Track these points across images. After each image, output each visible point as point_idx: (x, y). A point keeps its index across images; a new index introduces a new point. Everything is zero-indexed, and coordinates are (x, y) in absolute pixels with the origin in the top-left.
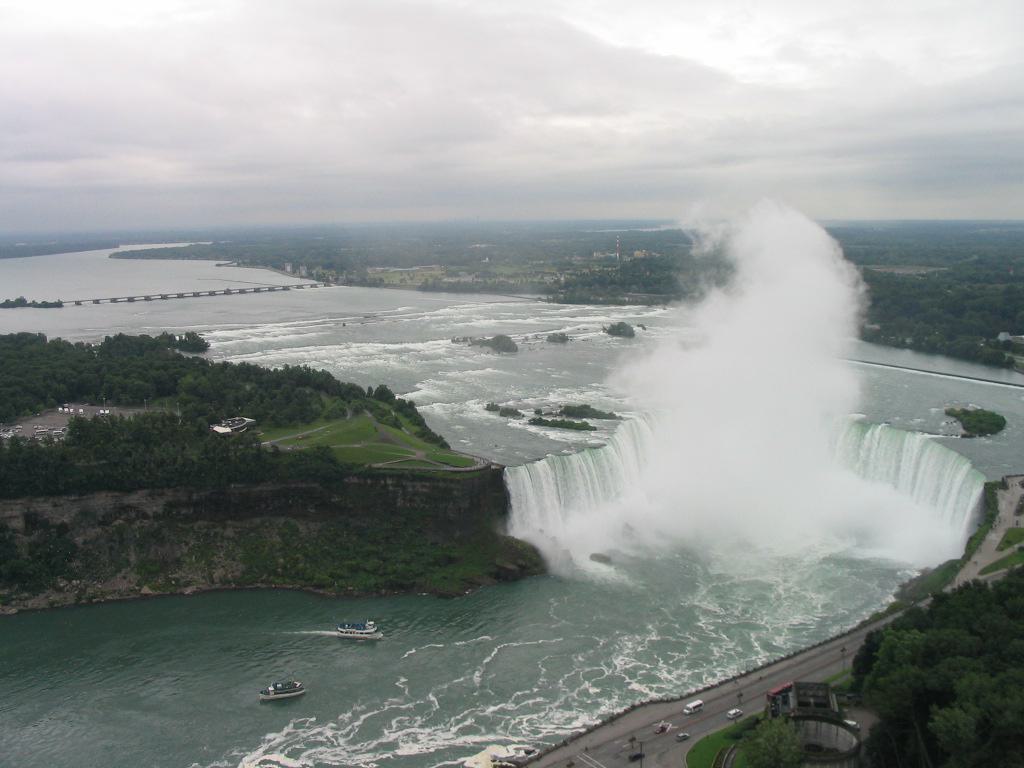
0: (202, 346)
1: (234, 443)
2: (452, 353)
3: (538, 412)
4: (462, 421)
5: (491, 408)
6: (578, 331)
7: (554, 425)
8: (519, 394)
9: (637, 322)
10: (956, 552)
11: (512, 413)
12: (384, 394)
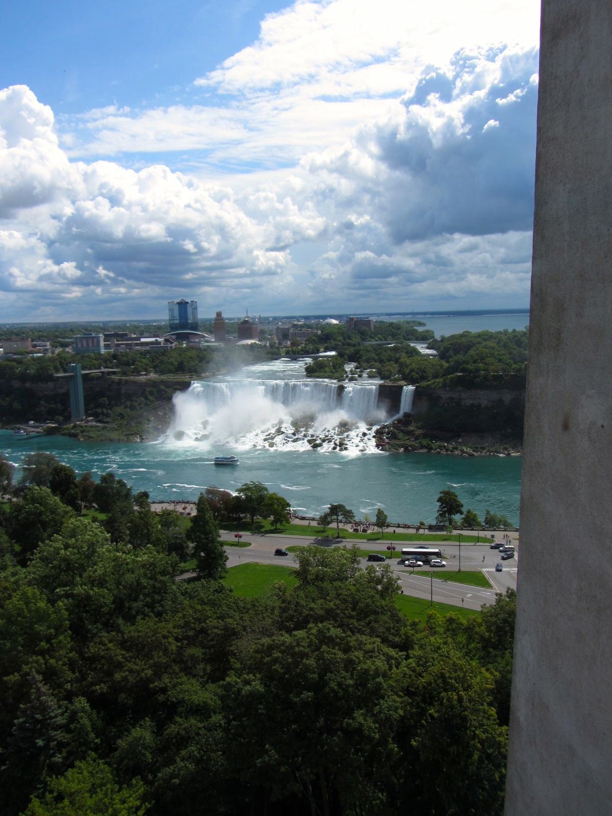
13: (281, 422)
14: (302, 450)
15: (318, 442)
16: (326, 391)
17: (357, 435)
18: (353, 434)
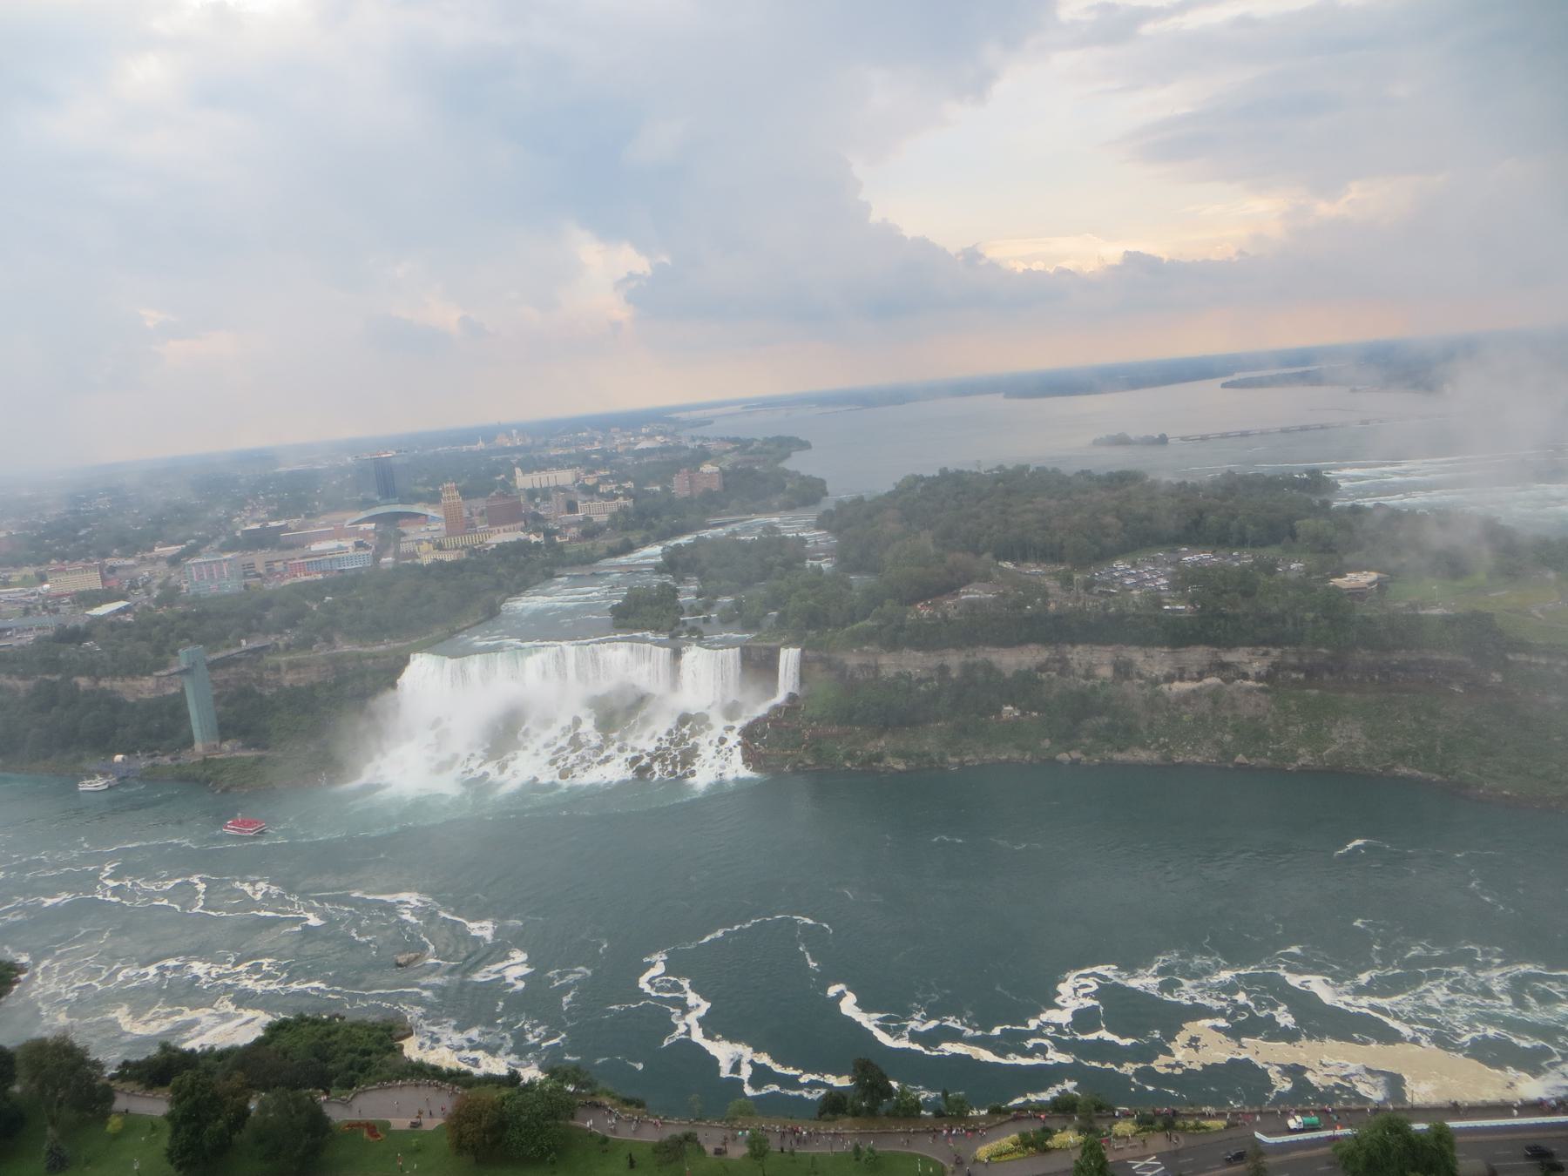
13: (577, 722)
14: (616, 778)
15: (643, 763)
16: (650, 660)
17: (710, 743)
18: (702, 740)
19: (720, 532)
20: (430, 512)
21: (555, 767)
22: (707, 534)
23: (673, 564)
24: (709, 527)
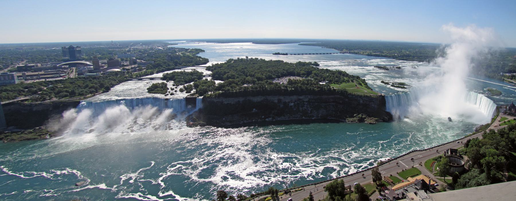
0: (318, 65)
1: (324, 86)
2: (373, 70)
3: (393, 84)
4: (376, 85)
5: (382, 82)
6: (403, 66)
7: (397, 87)
8: (389, 79)
9: (416, 65)
10: (489, 122)
11: (388, 84)
12: (358, 77)
19: (179, 70)
20: (88, 63)
21: (129, 129)
22: (176, 70)
23: (164, 78)
24: (176, 69)
